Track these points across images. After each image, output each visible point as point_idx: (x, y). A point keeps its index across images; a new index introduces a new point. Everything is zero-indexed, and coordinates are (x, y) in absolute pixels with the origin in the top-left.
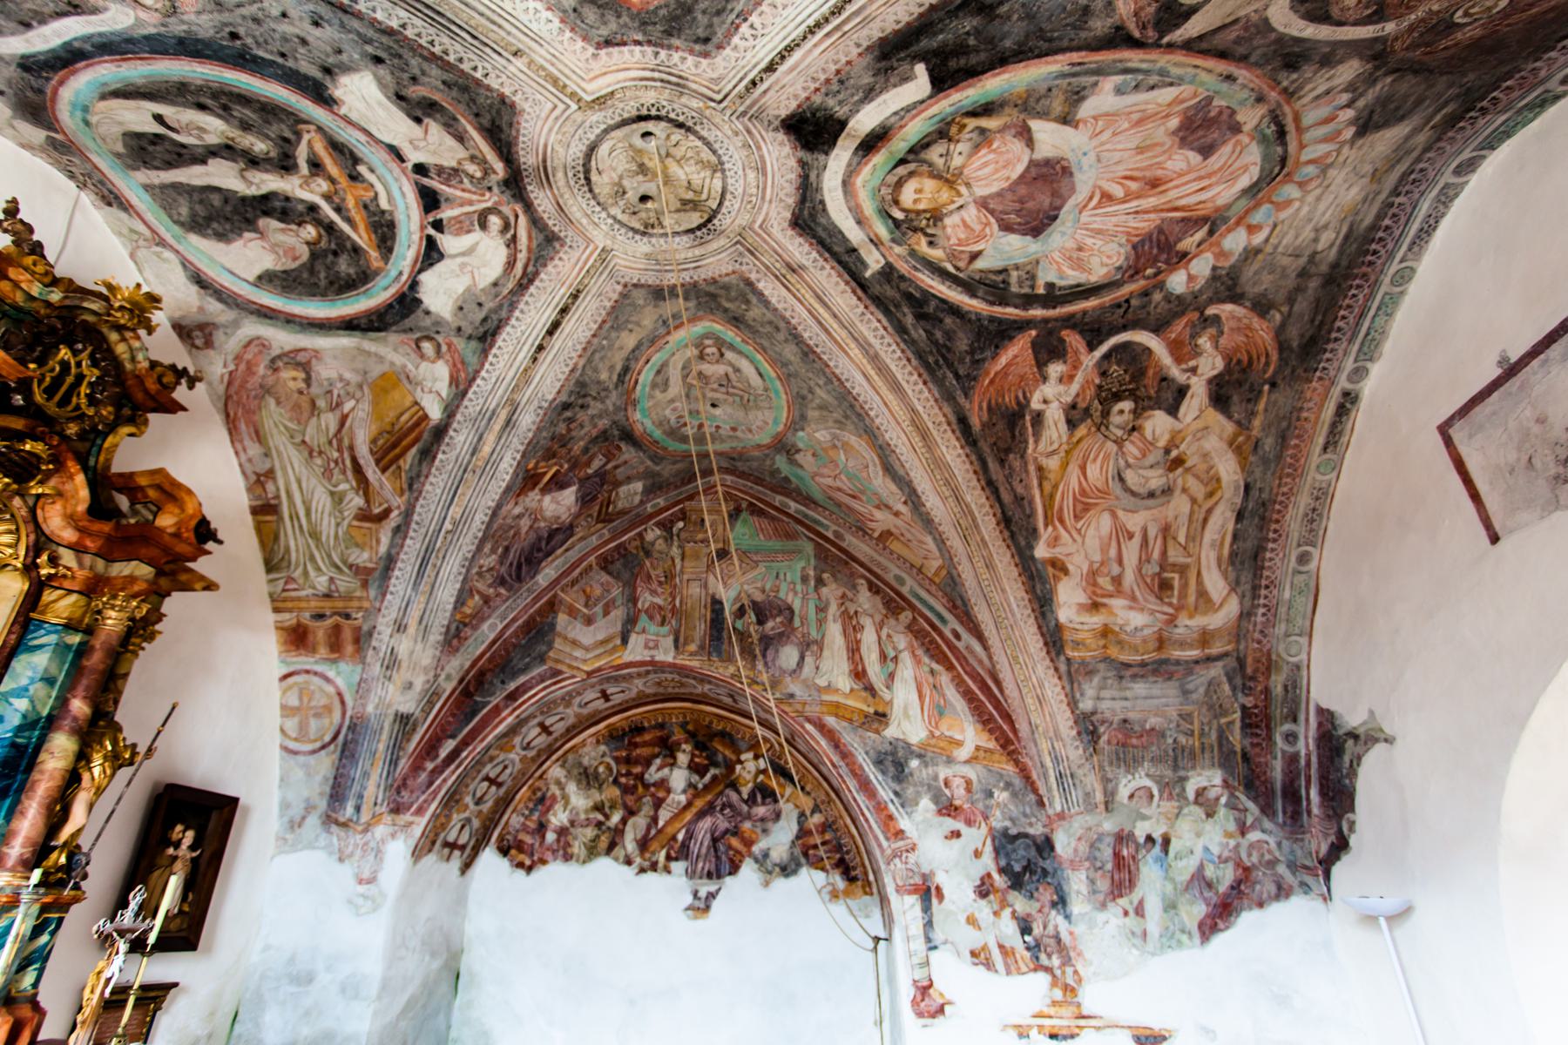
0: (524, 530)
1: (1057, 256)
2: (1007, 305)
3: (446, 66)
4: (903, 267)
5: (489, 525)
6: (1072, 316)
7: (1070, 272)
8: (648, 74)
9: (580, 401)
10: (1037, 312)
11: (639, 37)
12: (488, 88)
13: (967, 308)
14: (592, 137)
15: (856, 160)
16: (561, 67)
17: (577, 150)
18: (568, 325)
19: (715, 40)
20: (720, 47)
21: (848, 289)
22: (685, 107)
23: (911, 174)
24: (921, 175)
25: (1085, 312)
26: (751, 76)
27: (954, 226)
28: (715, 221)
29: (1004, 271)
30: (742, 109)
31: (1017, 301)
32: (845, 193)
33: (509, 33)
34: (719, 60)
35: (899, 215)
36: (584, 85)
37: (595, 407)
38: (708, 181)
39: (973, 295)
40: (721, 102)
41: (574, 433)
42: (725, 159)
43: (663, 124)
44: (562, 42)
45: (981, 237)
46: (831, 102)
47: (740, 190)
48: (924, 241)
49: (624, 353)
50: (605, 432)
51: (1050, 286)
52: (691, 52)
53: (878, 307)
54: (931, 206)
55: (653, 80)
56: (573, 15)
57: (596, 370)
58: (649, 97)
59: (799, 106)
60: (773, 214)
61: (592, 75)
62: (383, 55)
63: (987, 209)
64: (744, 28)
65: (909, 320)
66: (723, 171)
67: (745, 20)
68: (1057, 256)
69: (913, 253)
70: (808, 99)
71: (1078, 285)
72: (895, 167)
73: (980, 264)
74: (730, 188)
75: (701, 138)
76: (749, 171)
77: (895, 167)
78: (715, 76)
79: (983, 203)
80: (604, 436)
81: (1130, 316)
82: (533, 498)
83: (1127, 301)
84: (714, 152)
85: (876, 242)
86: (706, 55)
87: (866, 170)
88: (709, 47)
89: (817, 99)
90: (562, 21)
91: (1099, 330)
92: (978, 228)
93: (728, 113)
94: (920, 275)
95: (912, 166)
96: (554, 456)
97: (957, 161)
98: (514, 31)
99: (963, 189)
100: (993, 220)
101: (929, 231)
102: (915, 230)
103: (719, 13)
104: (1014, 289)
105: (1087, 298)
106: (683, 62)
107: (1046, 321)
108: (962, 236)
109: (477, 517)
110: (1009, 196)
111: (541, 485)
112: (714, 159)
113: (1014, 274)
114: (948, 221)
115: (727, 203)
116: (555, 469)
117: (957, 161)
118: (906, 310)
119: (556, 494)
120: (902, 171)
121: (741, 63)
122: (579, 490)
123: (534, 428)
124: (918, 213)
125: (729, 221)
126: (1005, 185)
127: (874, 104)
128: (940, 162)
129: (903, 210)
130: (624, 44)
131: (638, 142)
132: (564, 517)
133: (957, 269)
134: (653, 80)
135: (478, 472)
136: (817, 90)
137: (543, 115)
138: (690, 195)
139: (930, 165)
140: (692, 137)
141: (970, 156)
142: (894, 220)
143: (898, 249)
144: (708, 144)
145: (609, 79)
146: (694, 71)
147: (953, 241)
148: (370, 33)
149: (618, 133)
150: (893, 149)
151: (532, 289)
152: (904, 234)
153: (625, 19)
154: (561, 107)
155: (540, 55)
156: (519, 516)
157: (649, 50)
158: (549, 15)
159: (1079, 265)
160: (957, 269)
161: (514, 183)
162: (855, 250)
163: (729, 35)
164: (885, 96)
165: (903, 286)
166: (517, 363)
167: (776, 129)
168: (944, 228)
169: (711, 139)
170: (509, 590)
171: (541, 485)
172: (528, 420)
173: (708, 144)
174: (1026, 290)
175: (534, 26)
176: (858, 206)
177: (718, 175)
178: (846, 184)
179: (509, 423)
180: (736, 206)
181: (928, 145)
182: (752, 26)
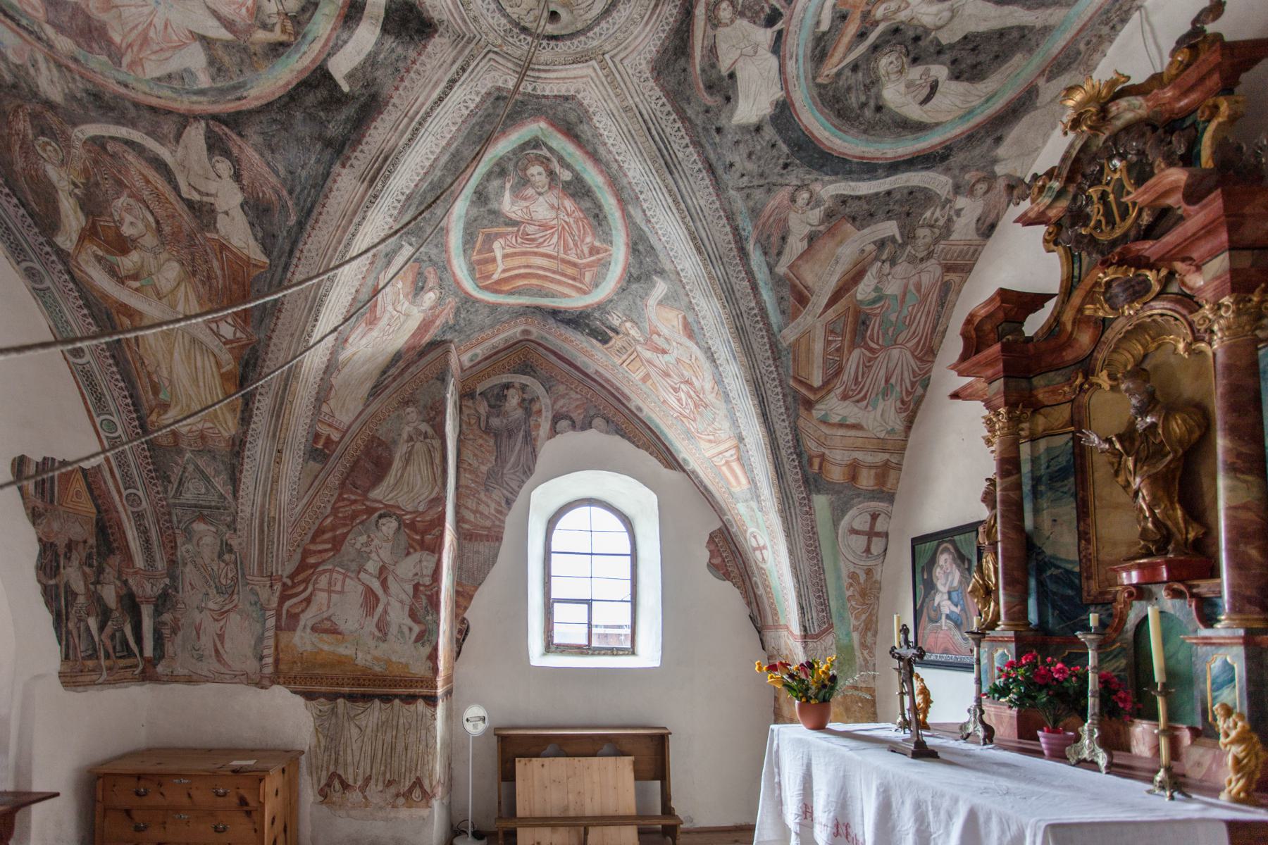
8: (543, 75)
19: (492, 99)
20: (489, 94)
26: (466, 75)
30: (472, 45)
34: (489, 85)
40: (489, 52)
44: (597, 107)
46: (400, 50)
55: (539, 70)
59: (425, 46)
61: (585, 79)
64: (472, 106)
67: (472, 111)
70: (419, 54)
75: (507, 16)
78: (493, 73)
86: (499, 89)
88: (496, 94)
89: (412, 54)
90: (591, 119)
93: (482, 43)
98: (623, 125)
103: (489, 115)
130: (556, 97)
134: (539, 70)
136: (414, 62)
140: (515, 17)
145: (571, 74)
146: (508, 77)
157: (539, 92)
158: (597, 124)
163: (483, 101)
175: (609, 122)
182: (467, 108)
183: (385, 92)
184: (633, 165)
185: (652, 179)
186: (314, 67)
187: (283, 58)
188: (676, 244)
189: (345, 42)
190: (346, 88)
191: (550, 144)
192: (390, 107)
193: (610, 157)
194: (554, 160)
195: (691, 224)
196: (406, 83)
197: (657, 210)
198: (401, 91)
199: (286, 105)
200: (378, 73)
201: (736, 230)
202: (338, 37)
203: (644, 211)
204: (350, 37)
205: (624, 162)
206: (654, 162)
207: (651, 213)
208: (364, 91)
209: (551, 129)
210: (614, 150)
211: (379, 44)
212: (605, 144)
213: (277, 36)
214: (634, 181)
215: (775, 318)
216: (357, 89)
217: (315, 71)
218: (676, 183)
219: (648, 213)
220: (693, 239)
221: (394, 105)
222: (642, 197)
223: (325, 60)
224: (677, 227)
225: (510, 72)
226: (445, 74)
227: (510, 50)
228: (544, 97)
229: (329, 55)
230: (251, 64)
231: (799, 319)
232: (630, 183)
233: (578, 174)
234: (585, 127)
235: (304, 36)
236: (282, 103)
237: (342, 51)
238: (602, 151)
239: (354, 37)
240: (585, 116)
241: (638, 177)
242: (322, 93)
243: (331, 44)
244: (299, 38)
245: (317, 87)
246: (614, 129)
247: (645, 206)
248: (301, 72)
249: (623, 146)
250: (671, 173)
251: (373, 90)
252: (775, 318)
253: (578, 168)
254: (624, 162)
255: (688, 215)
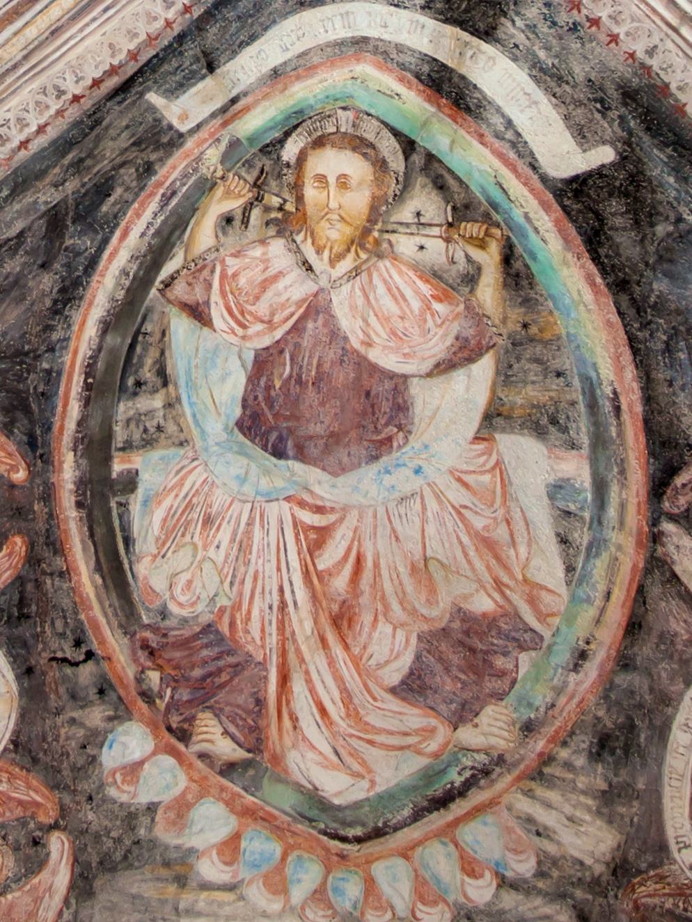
1: (196, 478)
2: (87, 402)
4: (172, 170)
6: (56, 545)
7: (159, 514)
10: (68, 470)
13: (77, 317)
15: (407, 59)
21: (122, 56)
23: (381, 165)
24: (378, 182)
25: (64, 574)
27: (265, 261)
29: (164, 377)
31: (94, 423)
32: (340, 44)
35: (290, 151)
39: (106, 327)
45: (240, 318)
48: (233, 205)
51: (130, 482)
53: (77, 124)
54: (310, 210)
63: (303, 318)
65: (45, 196)
68: (196, 478)
69: (206, 186)
71: (128, 541)
72: (396, 133)
73: (181, 327)
77: (396, 133)
79: (315, 308)
81: (54, 673)
83: (90, 655)
85: (230, 109)
87: (389, 82)
91: (24, 617)
92: (262, 308)
94: (153, 206)
95: (397, 163)
97: (405, 245)
99: (346, 264)
100: (278, 334)
101: (256, 213)
102: (258, 185)
104: (124, 409)
105: (98, 568)
107: (49, 495)
108: (242, 281)
110: (331, 355)
113: (157, 402)
114: (277, 247)
117: (405, 245)
118: (71, 186)
120: (389, 147)
124: (297, 188)
126: (355, 343)
127: (531, 86)
128: (406, 213)
129: (302, 158)
133: (167, 284)
139: (399, 198)
141: (416, 267)
142: (281, 142)
143: (213, 156)
147: (233, 264)
150: (436, 127)
152: (249, 164)
159: (174, 530)
160: (167, 284)
162: (211, 68)
164: (545, 104)
165: (128, 174)
168: (263, 242)
174: (120, 434)
176: (312, 69)
178: (361, 43)
181: (441, 187)
183: (624, 70)
186: (556, 206)
187: (534, 268)
189: (509, 123)
190: (605, 155)
192: (654, 63)
196: (603, 14)
198: (621, 30)
199: (639, 307)
200: (579, 71)
202: (498, 136)
204: (499, 110)
208: (614, 114)
211: (515, 53)
213: (489, 259)
216: (609, 128)
217: (564, 208)
221: (651, 52)
223: (544, 179)
229: (534, 167)
230: (546, 343)
235: (495, 206)
236: (632, 312)
237: (527, 137)
239: (500, 102)
242: (615, 209)
243: (512, 155)
244: (497, 217)
245: (599, 217)
248: (566, 240)
251: (613, 94)
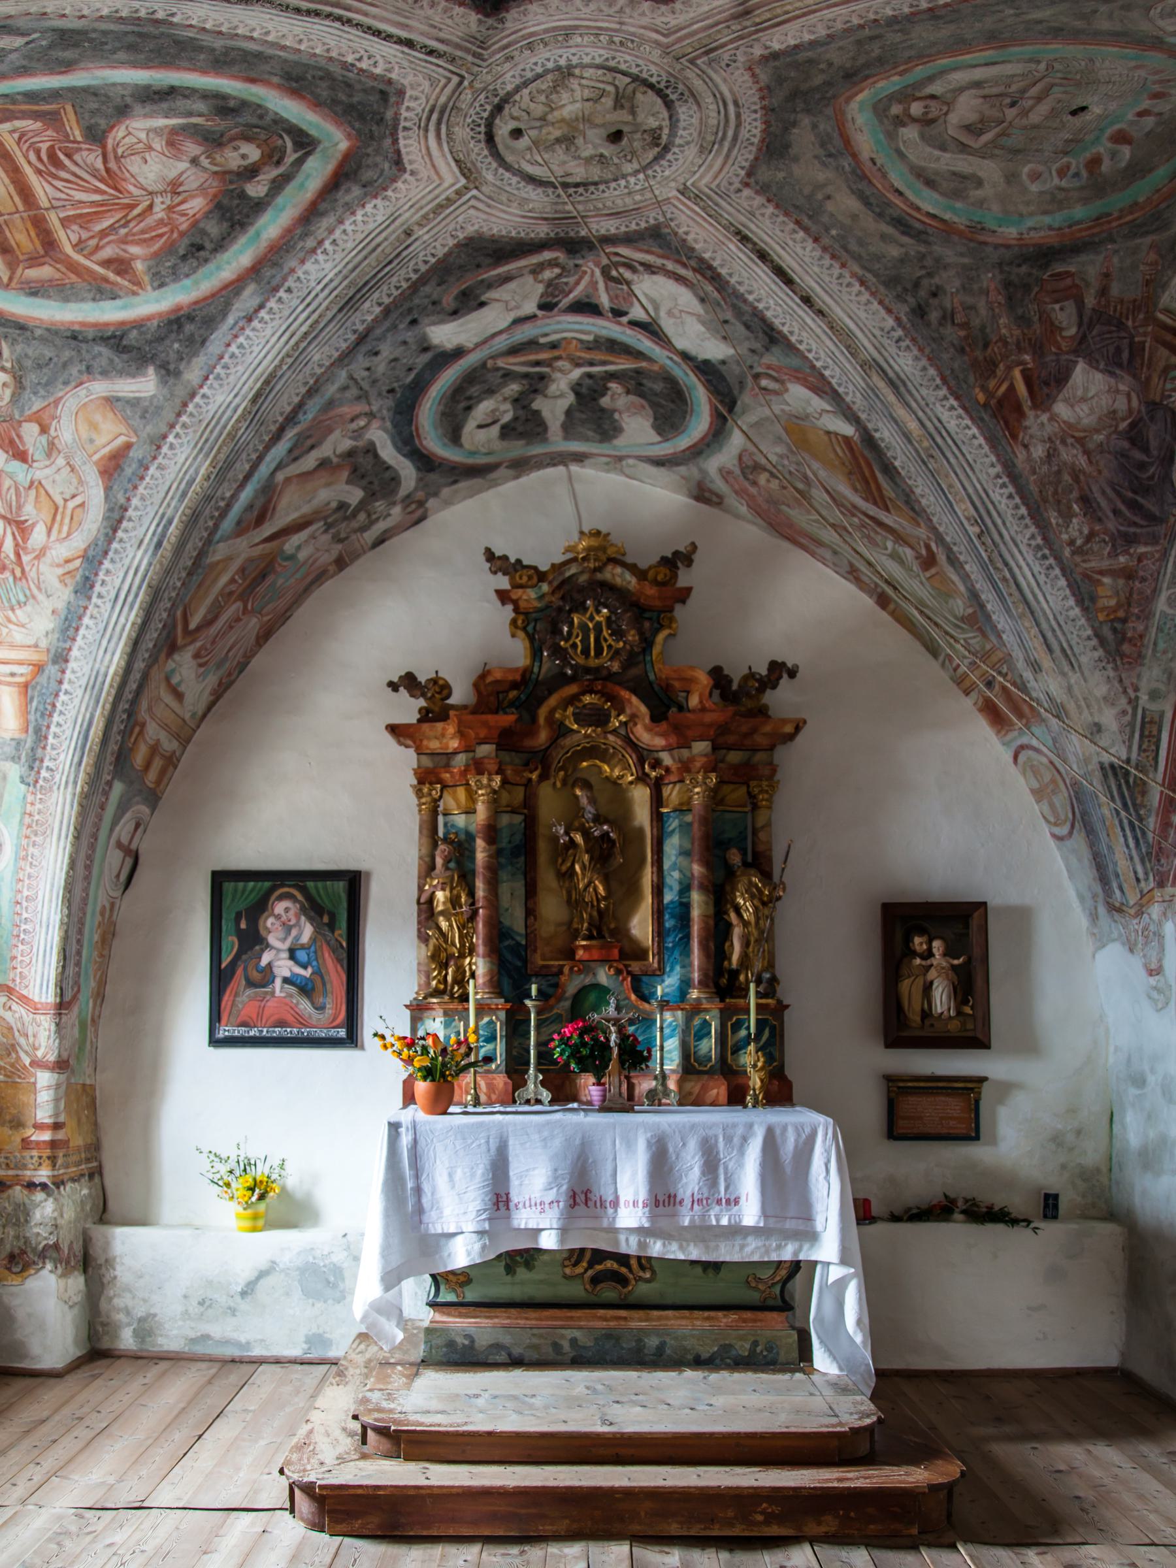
0: (1082, 461)
3: (423, 280)
5: (1022, 492)
9: (922, 293)
11: (389, 141)
12: (447, 255)
14: (515, 180)
16: (424, 202)
17: (533, 194)
18: (788, 261)
22: (474, 107)
28: (654, 80)
30: (470, 58)
33: (386, 239)
34: (406, 82)
36: (446, 185)
37: (950, 281)
38: (584, 82)
41: (976, 322)
42: (550, 65)
43: (497, 121)
47: (602, 52)
49: (869, 222)
50: (1007, 284)
52: (399, 104)
56: (369, 189)
57: (878, 258)
58: (462, 132)
60: (645, 21)
62: (409, 319)
66: (570, 67)
74: (598, 61)
76: (571, 43)
78: (427, 83)
80: (1014, 292)
82: (1036, 424)
84: (539, 76)
90: (375, 197)
93: (476, 69)
96: (992, 365)
98: (384, 235)
106: (412, 109)
109: (995, 497)
111: (1027, 403)
112: (550, 77)
115: (623, 67)
116: (1017, 373)
119: (1066, 392)
121: (405, 64)
122: (1093, 363)
123: (924, 362)
125: (653, 69)
130: (398, 152)
131: (524, 142)
132: (1121, 404)
135: (937, 453)
137: (484, 217)
138: (608, 102)
144: (526, 84)
146: (423, 100)
148: (387, 324)
149: (509, 158)
151: (723, 272)
153: (369, 150)
154: (473, 202)
155: (408, 217)
156: (1050, 455)
161: (575, 246)
166: (818, 331)
167: (502, 21)
169: (518, 81)
170: (1154, 540)
171: (1027, 403)
172: (906, 363)
173: (526, 84)
175: (380, 219)
177: (577, 71)
179: (896, 384)
180: (628, 58)
184: (329, 266)
185: (322, 296)
188: (240, 368)
191: (311, 158)
193: (321, 233)
194: (281, 170)
195: (285, 367)
197: (276, 323)
201: (300, 406)
203: (261, 306)
205: (325, 252)
206: (348, 287)
207: (267, 317)
209: (339, 156)
210: (337, 234)
212: (341, 222)
214: (300, 273)
215: (228, 524)
218: (330, 321)
219: (263, 313)
220: (267, 382)
222: (281, 293)
224: (270, 357)
225: (431, 102)
226: (422, 34)
227: (467, 96)
228: (395, 141)
231: (239, 540)
232: (293, 271)
233: (268, 204)
234: (356, 191)
238: (326, 222)
240: (374, 189)
241: (312, 277)
246: (371, 226)
247: (272, 304)
249: (350, 245)
250: (340, 310)
252: (228, 524)
253: (280, 200)
254: (325, 252)
255: (296, 355)
